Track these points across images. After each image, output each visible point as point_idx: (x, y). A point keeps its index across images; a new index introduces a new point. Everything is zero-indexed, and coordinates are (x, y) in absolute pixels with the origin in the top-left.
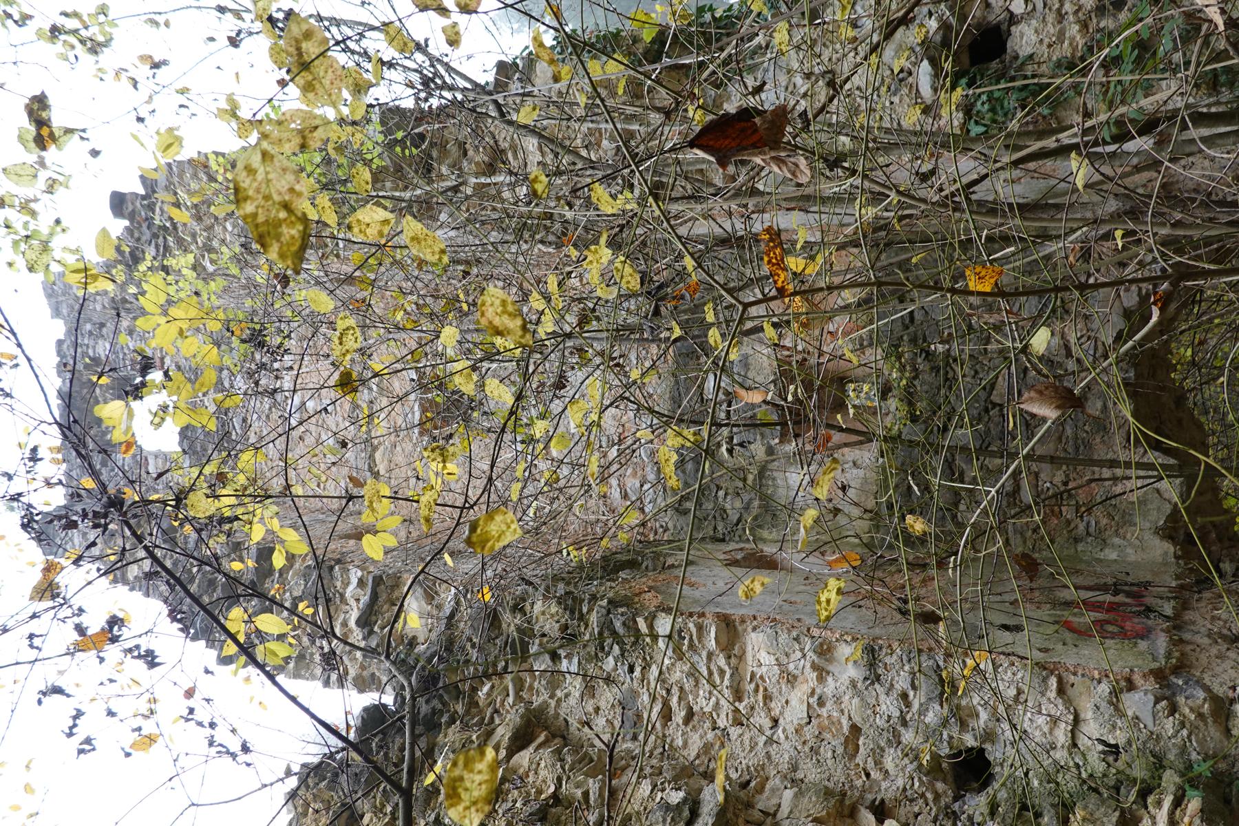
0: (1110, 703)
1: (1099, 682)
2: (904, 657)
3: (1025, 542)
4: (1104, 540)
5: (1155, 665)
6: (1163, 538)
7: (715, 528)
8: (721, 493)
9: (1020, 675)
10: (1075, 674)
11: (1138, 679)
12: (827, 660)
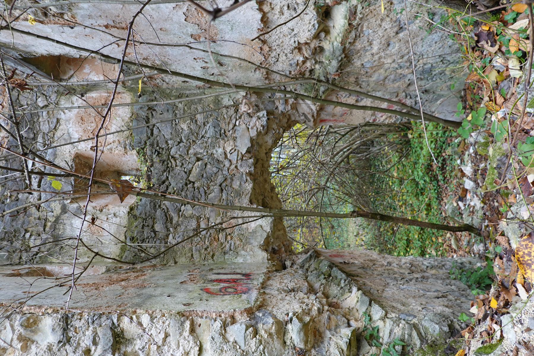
0: (221, 334)
1: (215, 320)
2: (90, 320)
3: (201, 256)
4: (237, 253)
5: (248, 306)
6: (263, 250)
7: (21, 258)
8: (28, 235)
9: (167, 322)
10: (202, 317)
11: (238, 316)
12: (32, 331)
